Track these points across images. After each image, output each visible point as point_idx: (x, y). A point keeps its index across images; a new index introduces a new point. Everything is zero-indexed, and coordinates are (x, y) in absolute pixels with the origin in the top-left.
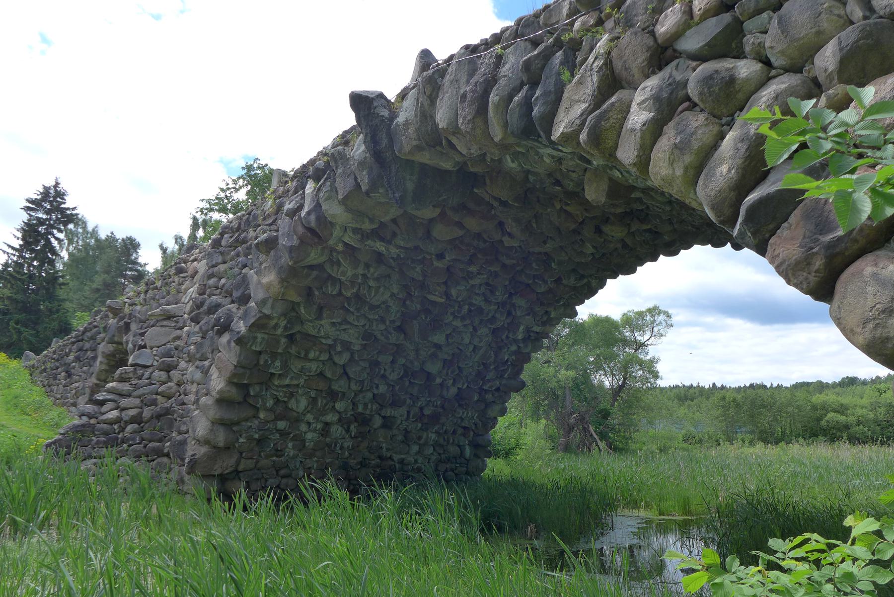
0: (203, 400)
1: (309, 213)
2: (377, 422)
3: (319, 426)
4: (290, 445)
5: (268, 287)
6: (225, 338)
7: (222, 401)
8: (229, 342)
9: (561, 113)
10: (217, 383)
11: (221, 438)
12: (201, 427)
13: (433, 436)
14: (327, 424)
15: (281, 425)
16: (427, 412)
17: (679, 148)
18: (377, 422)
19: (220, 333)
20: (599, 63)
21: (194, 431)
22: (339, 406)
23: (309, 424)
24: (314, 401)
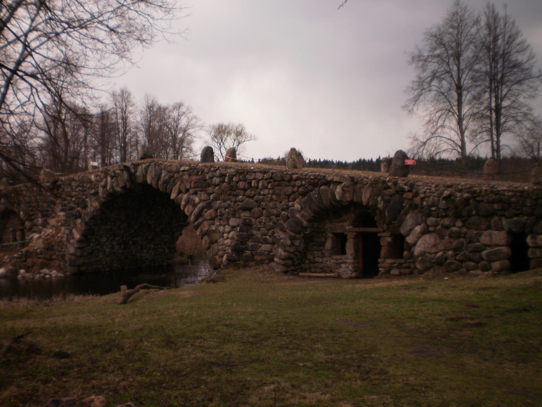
0: (72, 241)
1: (110, 189)
2: (131, 243)
3: (110, 246)
4: (101, 253)
5: (96, 207)
6: (79, 221)
7: (80, 241)
8: (81, 223)
9: (172, 194)
10: (77, 236)
11: (79, 253)
12: (72, 250)
13: (152, 246)
14: (113, 246)
15: (98, 247)
16: (150, 237)
17: (188, 211)
18: (131, 243)
19: (76, 218)
20: (178, 188)
21: (69, 251)
22: (117, 239)
23: (107, 246)
24: (108, 238)
